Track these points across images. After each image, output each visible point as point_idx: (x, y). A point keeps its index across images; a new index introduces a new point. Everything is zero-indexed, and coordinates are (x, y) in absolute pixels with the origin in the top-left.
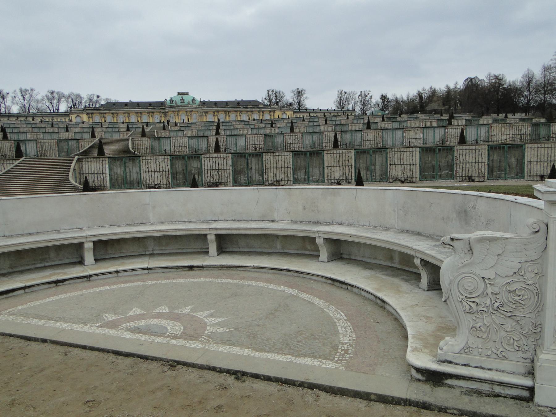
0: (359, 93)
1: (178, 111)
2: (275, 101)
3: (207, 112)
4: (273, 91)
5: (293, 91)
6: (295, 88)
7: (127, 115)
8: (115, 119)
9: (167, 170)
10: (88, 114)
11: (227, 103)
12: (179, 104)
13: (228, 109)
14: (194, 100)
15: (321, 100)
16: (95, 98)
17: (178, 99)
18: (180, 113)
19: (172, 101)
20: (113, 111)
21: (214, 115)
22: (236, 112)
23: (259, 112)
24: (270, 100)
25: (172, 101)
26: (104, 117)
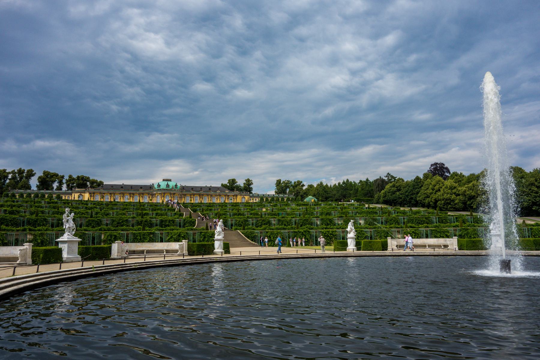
1: (164, 194)
10: (90, 193)
11: (201, 188)
13: (201, 192)
14: (176, 185)
17: (163, 185)
20: (111, 191)
21: (191, 198)
22: (208, 195)
23: (225, 196)
25: (159, 186)
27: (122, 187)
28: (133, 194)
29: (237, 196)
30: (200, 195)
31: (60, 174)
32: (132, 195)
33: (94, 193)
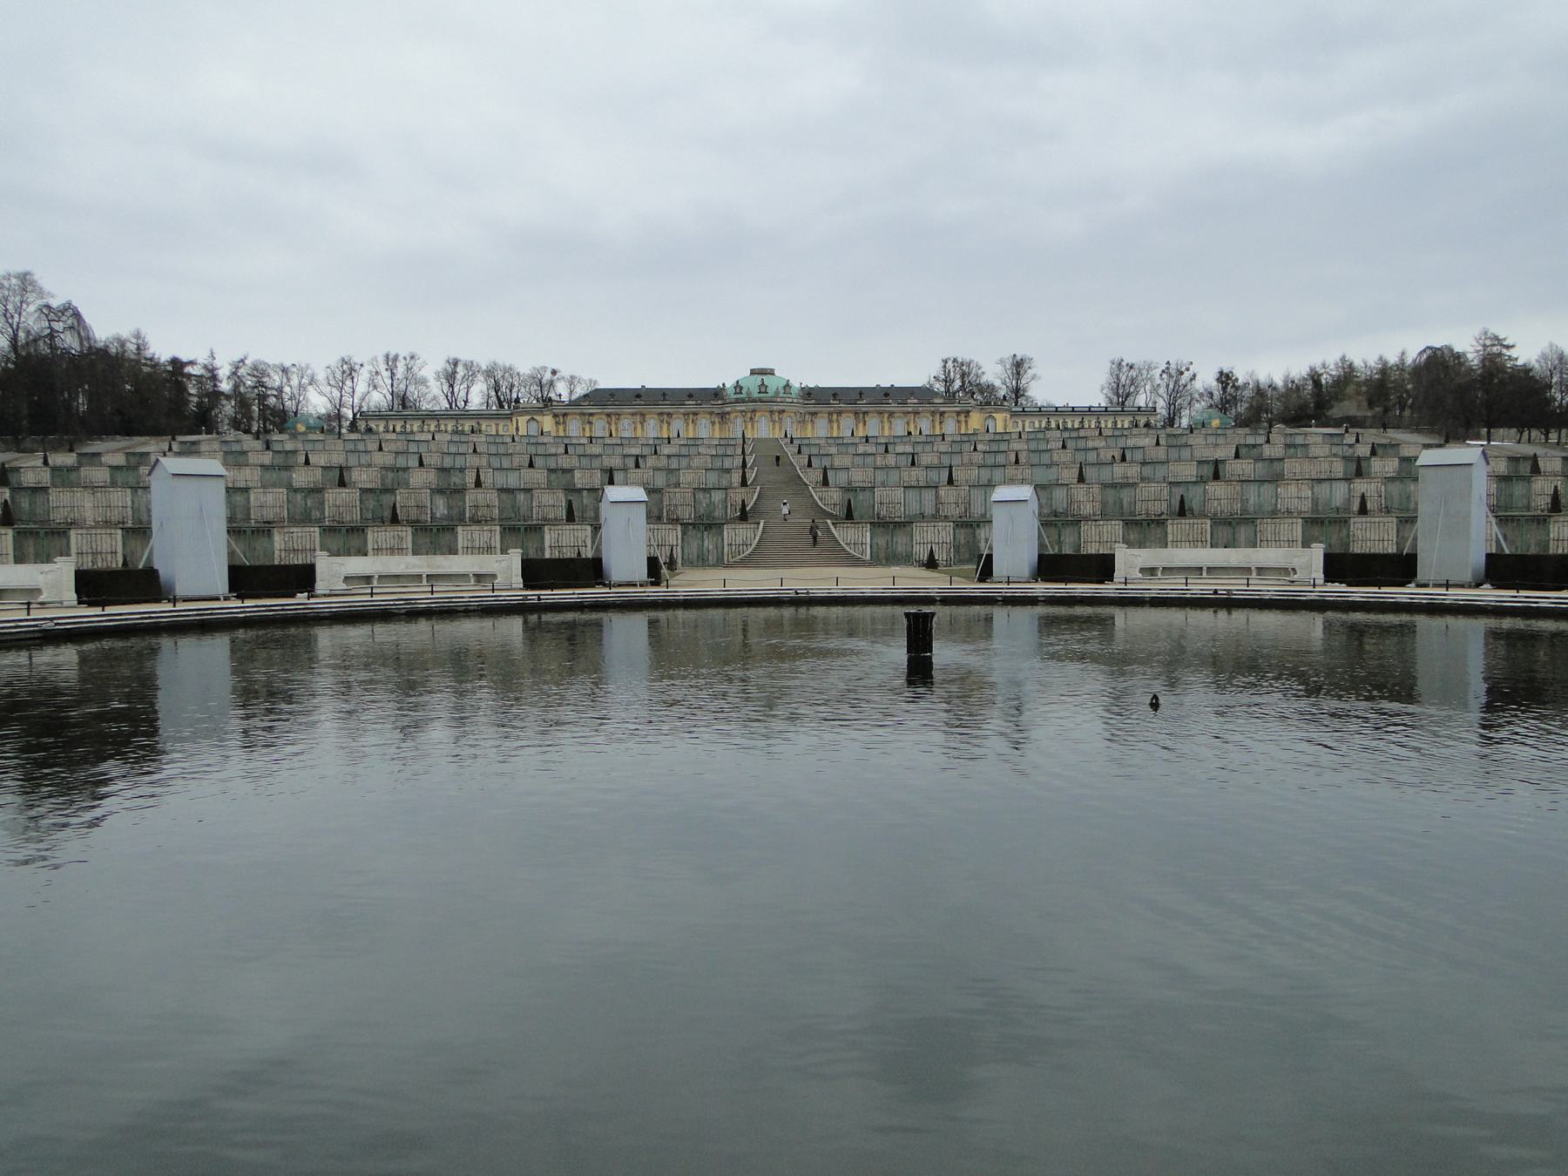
0: (1164, 366)
1: (754, 411)
2: (961, 391)
3: (814, 414)
4: (955, 360)
5: (1001, 361)
6: (1007, 354)
7: (638, 418)
10: (555, 416)
11: (861, 392)
12: (756, 395)
14: (787, 386)
15: (1069, 381)
16: (548, 376)
17: (752, 385)
19: (738, 387)
21: (831, 421)
22: (880, 413)
23: (933, 413)
24: (948, 381)
27: (638, 396)
28: (669, 414)
33: (565, 415)
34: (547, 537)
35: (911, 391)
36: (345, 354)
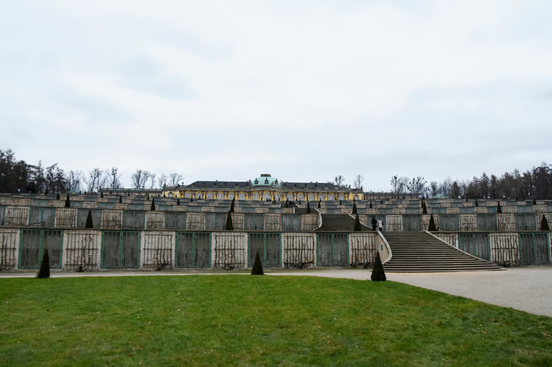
1: (263, 191)
7: (215, 193)
8: (316, 198)
9: (515, 247)
10: (180, 191)
11: (306, 185)
13: (306, 190)
14: (276, 181)
17: (262, 181)
18: (265, 192)
19: (256, 181)
21: (294, 196)
22: (314, 193)
23: (335, 193)
25: (256, 181)
26: (195, 195)
28: (228, 192)
29: (348, 194)
30: (304, 193)
31: (152, 172)
32: (226, 193)
33: (184, 191)
34: (213, 241)
35: (326, 185)
36: (96, 168)
